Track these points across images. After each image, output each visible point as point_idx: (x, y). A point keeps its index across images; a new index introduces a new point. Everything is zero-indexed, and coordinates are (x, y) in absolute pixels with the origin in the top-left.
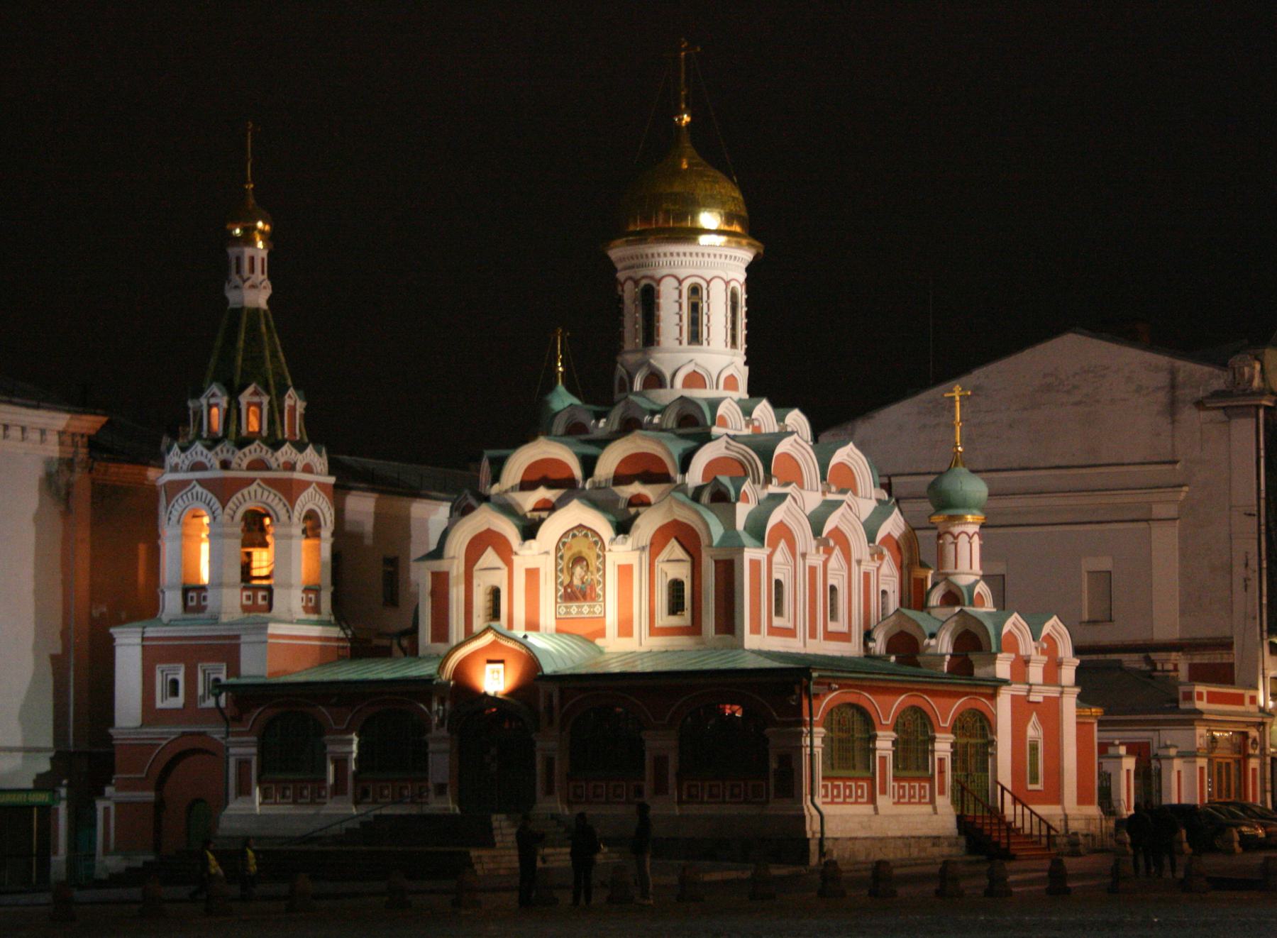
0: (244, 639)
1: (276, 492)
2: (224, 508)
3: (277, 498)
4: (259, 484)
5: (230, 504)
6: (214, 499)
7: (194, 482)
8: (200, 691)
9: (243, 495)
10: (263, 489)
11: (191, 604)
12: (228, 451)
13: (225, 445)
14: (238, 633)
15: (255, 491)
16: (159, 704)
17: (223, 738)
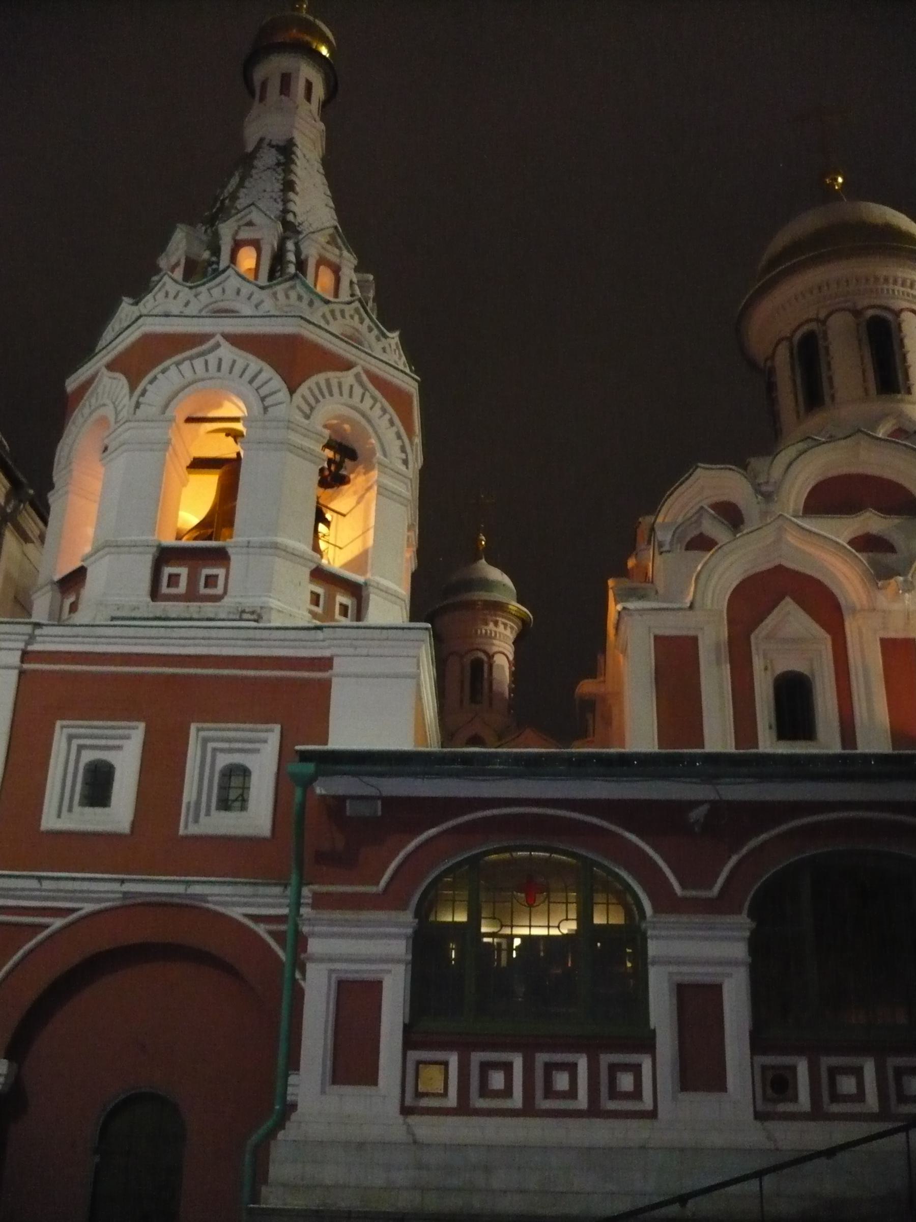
0: (339, 665)
1: (390, 409)
2: (292, 391)
3: (387, 417)
4: (357, 376)
5: (303, 389)
6: (268, 372)
7: (218, 338)
8: (189, 794)
9: (328, 382)
10: (366, 389)
11: (164, 589)
12: (300, 298)
13: (293, 287)
14: (327, 653)
15: (351, 387)
16: (50, 821)
17: (257, 918)
